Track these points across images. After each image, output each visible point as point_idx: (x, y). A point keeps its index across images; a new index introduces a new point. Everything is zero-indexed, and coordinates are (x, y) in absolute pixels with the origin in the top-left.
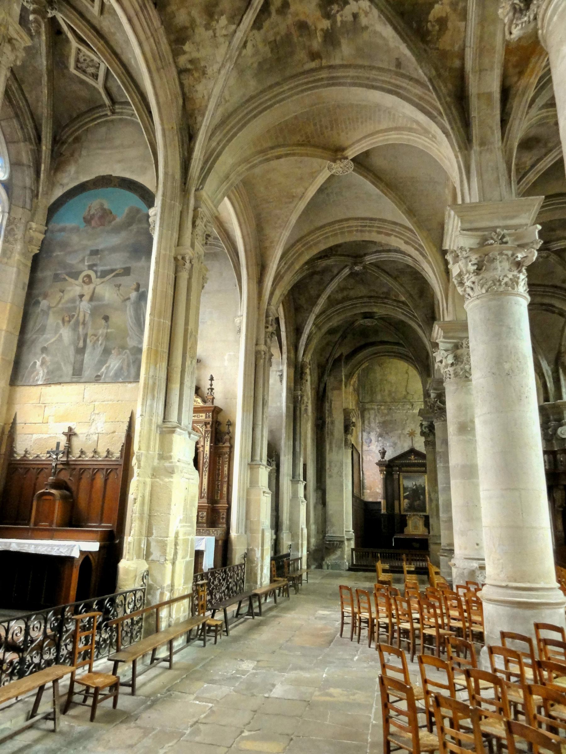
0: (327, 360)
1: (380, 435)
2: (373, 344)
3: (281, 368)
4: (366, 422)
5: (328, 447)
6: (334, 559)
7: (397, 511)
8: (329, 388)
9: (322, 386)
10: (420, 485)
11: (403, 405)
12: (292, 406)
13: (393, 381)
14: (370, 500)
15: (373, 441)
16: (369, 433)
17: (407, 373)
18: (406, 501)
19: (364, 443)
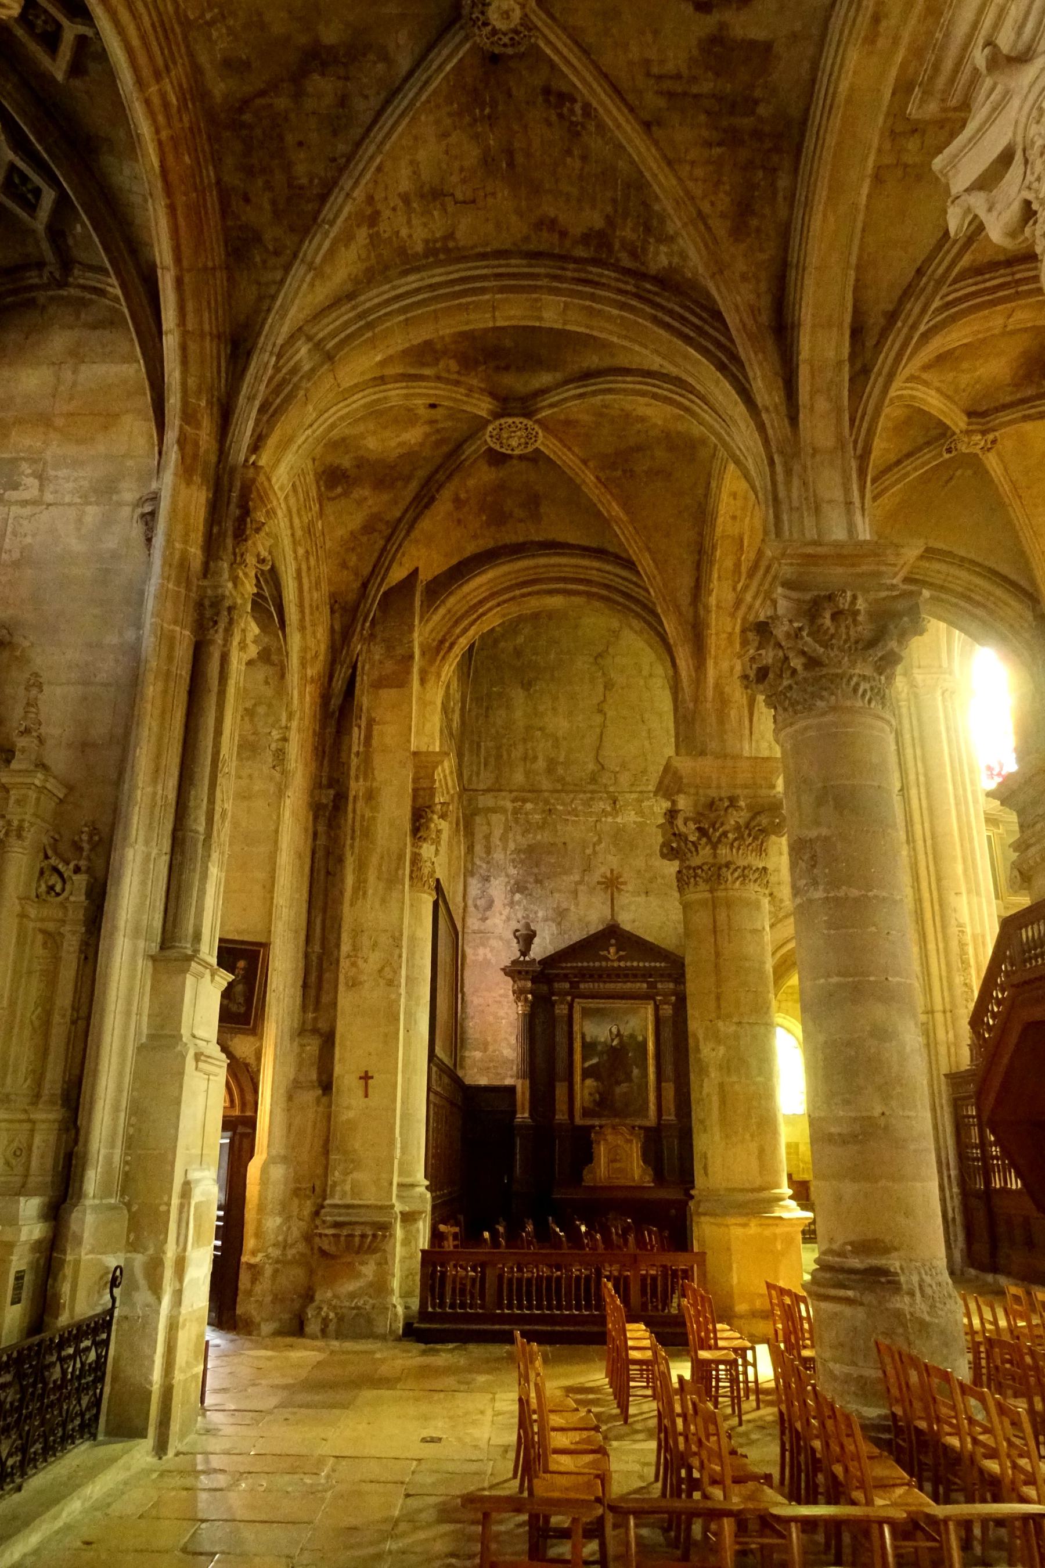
0: (365, 585)
1: (519, 887)
2: (516, 550)
3: (154, 486)
4: (479, 848)
5: (350, 880)
6: (352, 1296)
7: (561, 1116)
8: (363, 682)
9: (341, 675)
10: (632, 1036)
11: (587, 803)
12: (185, 637)
13: (560, 734)
14: (483, 1081)
15: (498, 904)
16: (487, 879)
17: (600, 711)
18: (589, 1082)
19: (471, 909)
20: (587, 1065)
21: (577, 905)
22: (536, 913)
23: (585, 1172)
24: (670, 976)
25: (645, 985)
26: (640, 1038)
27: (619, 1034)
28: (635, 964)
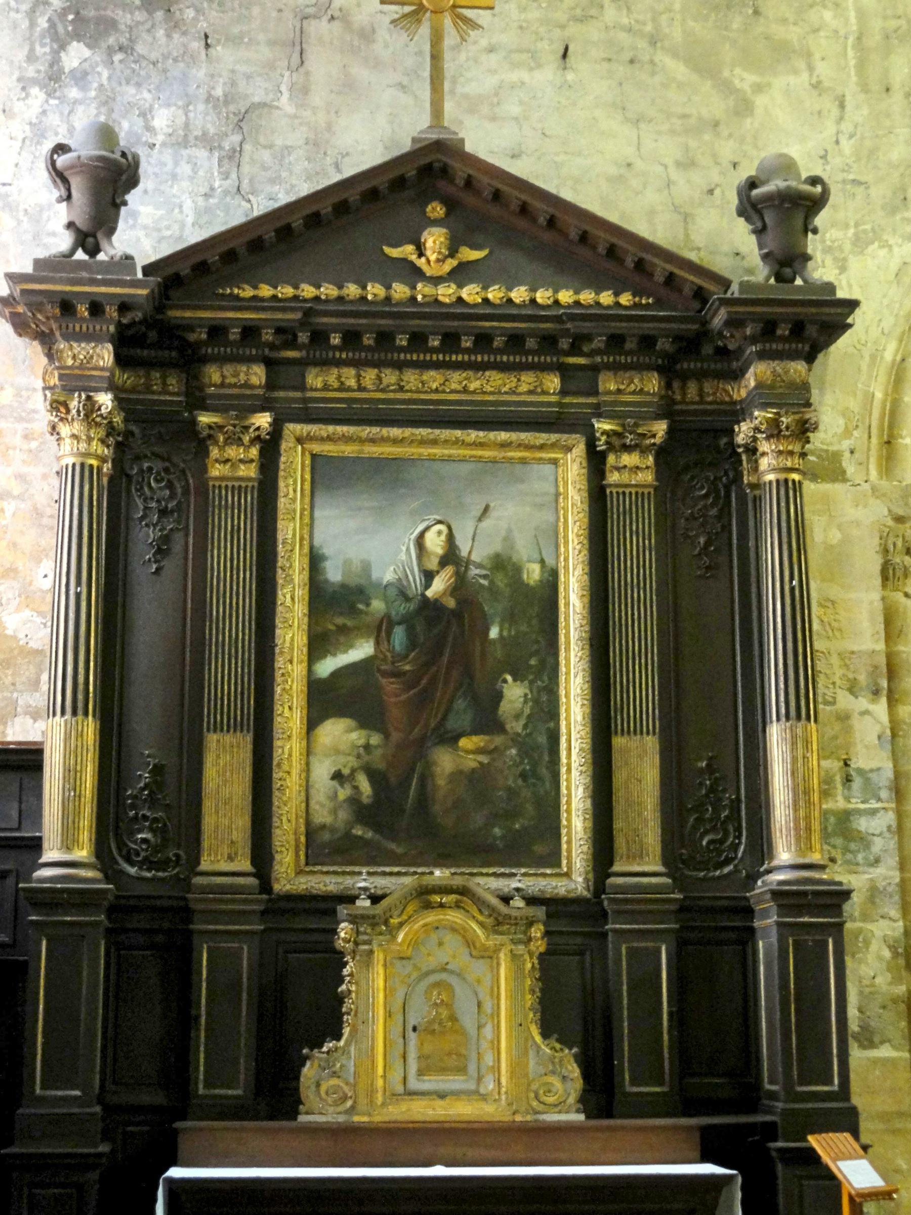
20: (327, 667)
21: (302, 91)
22: (145, 114)
23: (308, 1071)
24: (647, 342)
25: (553, 382)
26: (533, 573)
27: (451, 556)
28: (519, 294)
